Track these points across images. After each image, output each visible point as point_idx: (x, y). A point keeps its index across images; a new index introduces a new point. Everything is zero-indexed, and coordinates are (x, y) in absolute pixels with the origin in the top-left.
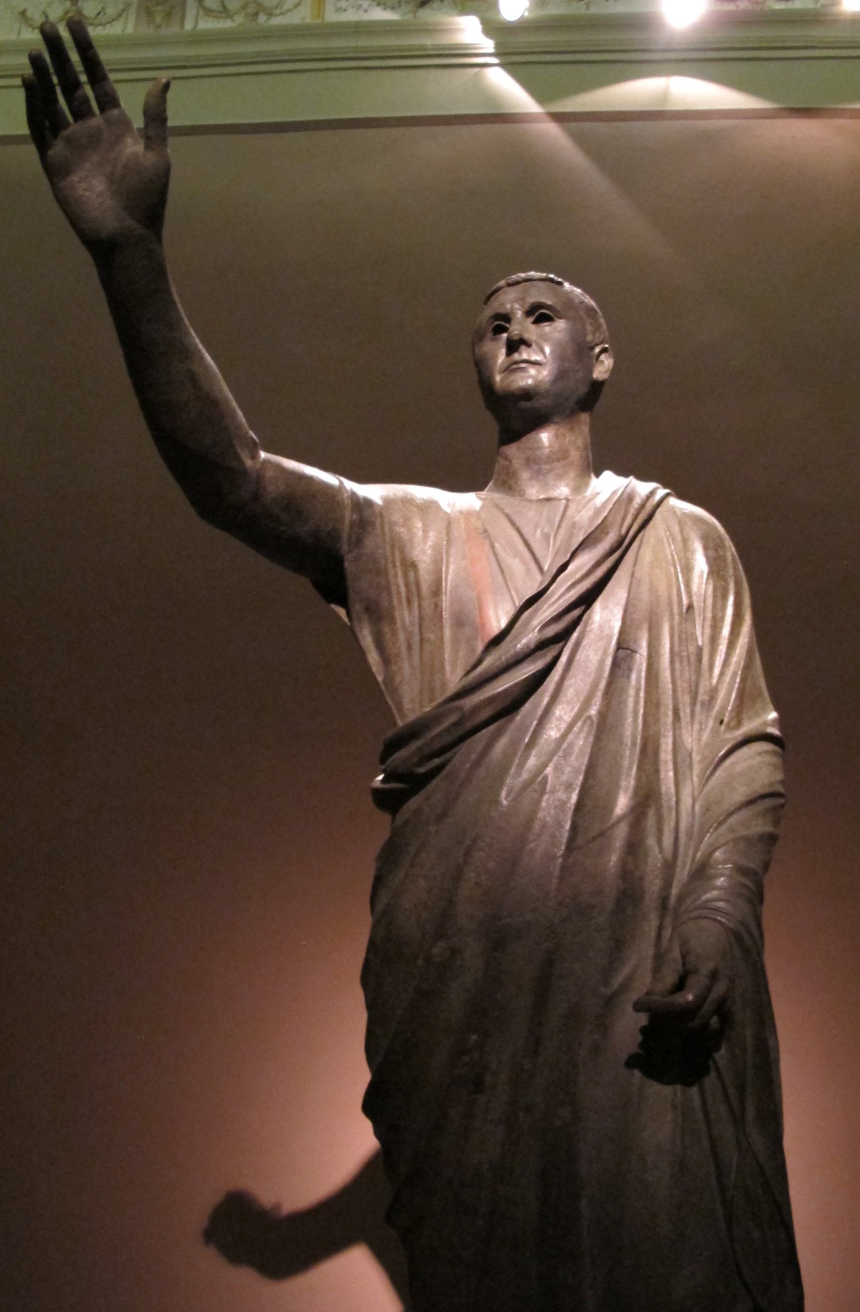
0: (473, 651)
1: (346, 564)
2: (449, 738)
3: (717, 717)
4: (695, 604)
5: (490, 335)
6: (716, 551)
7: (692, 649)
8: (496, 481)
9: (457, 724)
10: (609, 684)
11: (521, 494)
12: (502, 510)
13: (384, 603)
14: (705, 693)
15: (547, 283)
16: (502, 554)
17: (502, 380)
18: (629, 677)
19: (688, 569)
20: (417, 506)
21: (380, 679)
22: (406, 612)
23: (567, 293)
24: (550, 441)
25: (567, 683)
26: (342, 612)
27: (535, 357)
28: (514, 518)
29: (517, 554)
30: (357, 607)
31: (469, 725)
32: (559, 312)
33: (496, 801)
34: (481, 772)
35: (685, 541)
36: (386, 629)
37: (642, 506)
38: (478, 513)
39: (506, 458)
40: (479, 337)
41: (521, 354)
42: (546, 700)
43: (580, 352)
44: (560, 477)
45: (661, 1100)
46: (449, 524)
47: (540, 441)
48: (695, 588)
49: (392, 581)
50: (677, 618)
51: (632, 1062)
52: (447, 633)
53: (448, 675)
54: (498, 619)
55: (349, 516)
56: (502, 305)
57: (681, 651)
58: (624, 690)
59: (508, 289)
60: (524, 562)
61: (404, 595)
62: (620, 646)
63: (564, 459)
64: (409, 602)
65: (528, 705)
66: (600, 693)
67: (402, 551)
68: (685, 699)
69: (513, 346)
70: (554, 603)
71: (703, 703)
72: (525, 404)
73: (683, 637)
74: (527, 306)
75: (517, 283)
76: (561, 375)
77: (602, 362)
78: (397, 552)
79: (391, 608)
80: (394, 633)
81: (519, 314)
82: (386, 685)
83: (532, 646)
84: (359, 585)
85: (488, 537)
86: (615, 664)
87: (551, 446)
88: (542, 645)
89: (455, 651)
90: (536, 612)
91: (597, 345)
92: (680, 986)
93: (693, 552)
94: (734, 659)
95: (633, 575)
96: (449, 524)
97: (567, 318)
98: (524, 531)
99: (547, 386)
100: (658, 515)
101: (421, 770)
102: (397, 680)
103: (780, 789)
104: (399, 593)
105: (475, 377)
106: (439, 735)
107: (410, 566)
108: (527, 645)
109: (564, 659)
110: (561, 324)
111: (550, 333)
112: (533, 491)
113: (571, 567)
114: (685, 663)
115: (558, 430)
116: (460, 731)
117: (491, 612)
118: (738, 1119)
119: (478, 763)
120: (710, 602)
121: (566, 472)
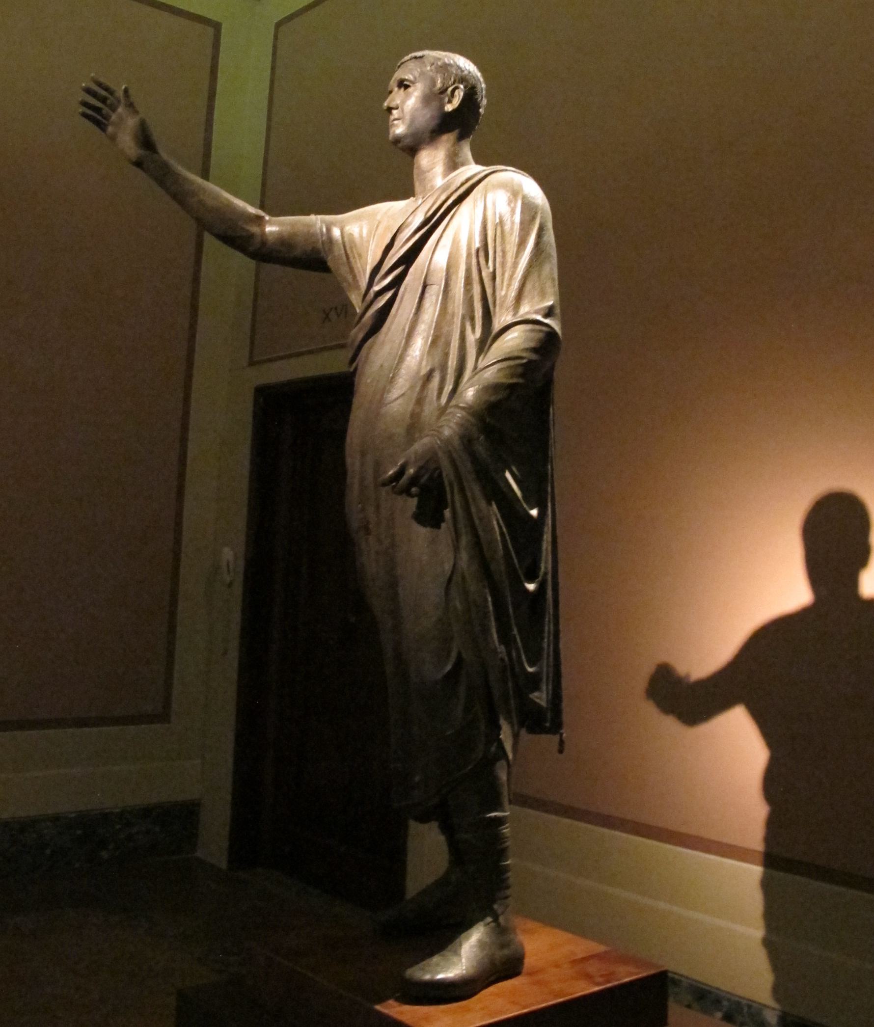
43: (436, 96)
45: (422, 532)
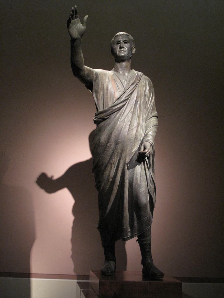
0: (113, 100)
1: (93, 84)
2: (111, 113)
3: (148, 112)
4: (147, 94)
5: (116, 44)
8: (114, 70)
9: (112, 111)
11: (120, 73)
12: (117, 76)
13: (98, 91)
19: (146, 88)
24: (125, 64)
26: (90, 91)
27: (124, 50)
29: (120, 84)
30: (94, 91)
31: (114, 112)
33: (117, 123)
34: (115, 119)
36: (98, 95)
39: (117, 66)
40: (114, 44)
42: (125, 109)
43: (131, 49)
44: (126, 70)
47: (123, 64)
48: (147, 91)
51: (136, 160)
53: (109, 103)
54: (117, 95)
55: (95, 76)
60: (121, 86)
61: (101, 89)
62: (136, 101)
64: (102, 90)
66: (133, 108)
67: (101, 82)
68: (144, 109)
69: (121, 48)
72: (122, 58)
73: (144, 100)
76: (129, 53)
79: (99, 92)
81: (122, 41)
84: (95, 88)
86: (135, 104)
88: (125, 100)
89: (110, 100)
92: (144, 149)
94: (152, 103)
97: (130, 43)
101: (106, 118)
103: (157, 124)
106: (109, 113)
109: (128, 102)
110: (129, 44)
116: (112, 112)
117: (116, 94)
118: (149, 170)
119: (115, 117)
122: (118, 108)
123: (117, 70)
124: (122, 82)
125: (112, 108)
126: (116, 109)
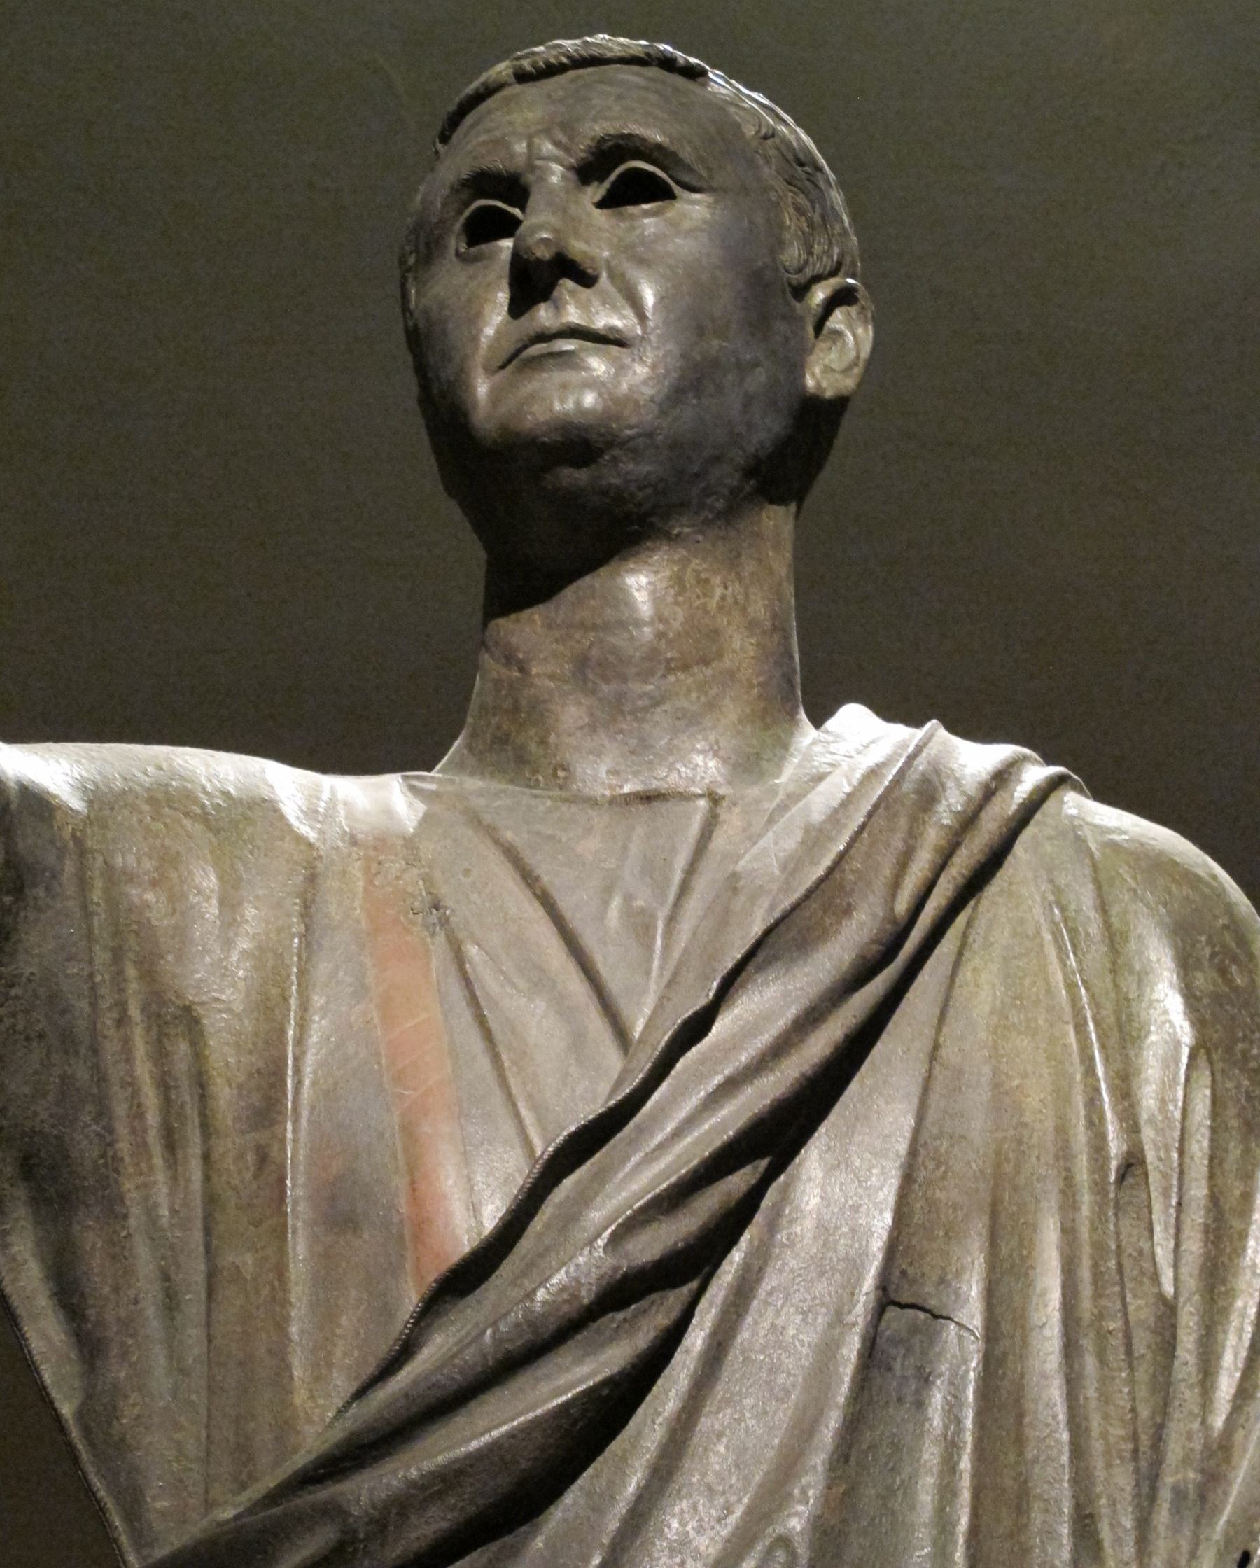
0: (387, 1311)
3: (1228, 1541)
5: (455, 243)
6: (1223, 972)
7: (1141, 1309)
8: (474, 735)
10: (854, 1424)
11: (560, 775)
12: (491, 832)
13: (85, 1149)
14: (1186, 1461)
15: (653, 72)
16: (489, 981)
17: (496, 396)
18: (920, 1405)
19: (1124, 1033)
20: (204, 818)
21: (66, 1410)
22: (161, 1177)
23: (720, 107)
24: (657, 600)
25: (705, 1423)
28: (533, 860)
29: (541, 982)
32: (689, 169)
35: (1115, 939)
36: (91, 1238)
37: (968, 821)
38: (410, 843)
39: (509, 658)
40: (424, 248)
41: (558, 308)
44: (690, 721)
46: (312, 879)
47: (623, 599)
48: (1148, 1098)
49: (115, 1073)
50: (1086, 1199)
52: (300, 1249)
53: (300, 1397)
54: (471, 1205)
56: (501, 143)
57: (1100, 1316)
58: (900, 1452)
59: (518, 88)
61: (153, 1118)
62: (886, 1300)
63: (706, 662)
64: (171, 1144)
65: (572, 1498)
66: (818, 1459)
67: (149, 974)
69: (533, 282)
70: (662, 1147)
71: (1179, 1494)
72: (572, 477)
73: (1104, 1268)
74: (582, 148)
75: (551, 71)
76: (693, 379)
77: (838, 334)
78: (131, 972)
80: (119, 1252)
81: (556, 174)
82: (86, 1430)
83: (586, 1297)
85: (444, 922)
86: (873, 1355)
87: (660, 617)
88: (622, 1293)
89: (326, 1314)
90: (600, 1178)
91: (817, 279)
93: (1143, 977)
95: (934, 1055)
96: (312, 879)
98: (565, 904)
99: (649, 417)
100: (1019, 848)
102: (128, 1413)
104: (138, 1114)
105: (408, 384)
107: (178, 1020)
108: (570, 1290)
110: (694, 208)
111: (659, 237)
112: (602, 771)
113: (721, 1027)
114: (1117, 1356)
115: (684, 562)
117: (448, 1180)
120: (1200, 1146)
121: (712, 706)
122: (448, 1480)
123: (517, 749)
124: (589, 940)
125: (323, 1494)
126: (403, 1506)
